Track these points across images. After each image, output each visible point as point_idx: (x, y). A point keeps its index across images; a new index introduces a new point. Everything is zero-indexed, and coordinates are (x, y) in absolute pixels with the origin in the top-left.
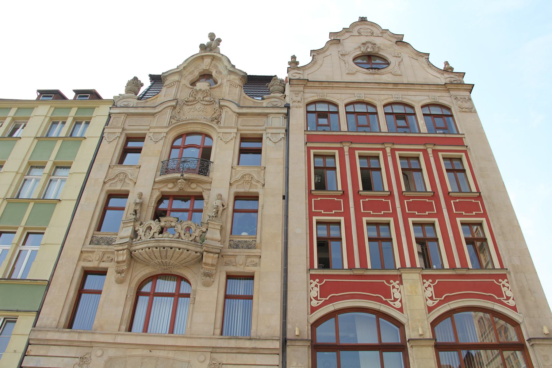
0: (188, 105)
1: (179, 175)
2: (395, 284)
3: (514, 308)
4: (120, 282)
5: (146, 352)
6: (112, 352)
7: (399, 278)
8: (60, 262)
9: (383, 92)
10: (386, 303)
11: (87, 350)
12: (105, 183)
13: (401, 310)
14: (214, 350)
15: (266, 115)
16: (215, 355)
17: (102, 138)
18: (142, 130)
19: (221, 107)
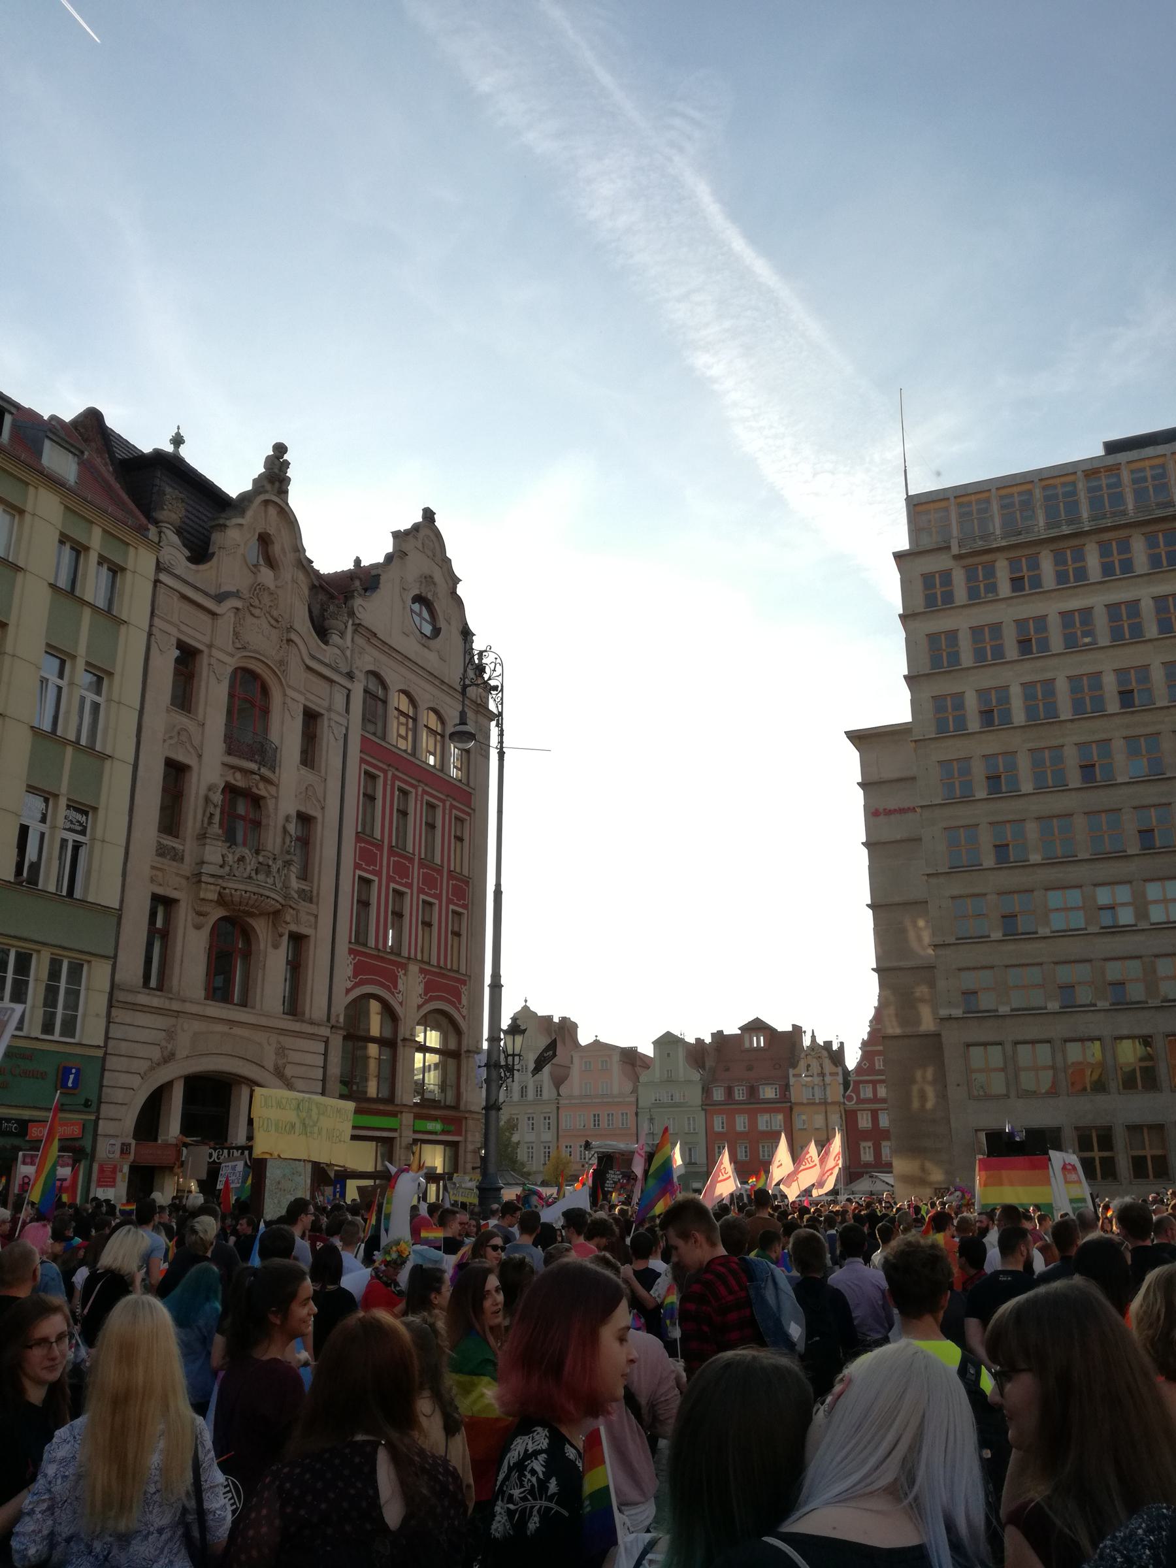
0: (252, 615)
1: (253, 766)
2: (402, 973)
3: (464, 1017)
4: (198, 927)
5: (224, 1028)
6: (197, 1026)
7: (404, 967)
8: (128, 880)
9: (428, 687)
10: (393, 994)
11: (172, 1021)
12: (164, 741)
13: (401, 1003)
14: (283, 1032)
15: (331, 681)
16: (281, 1038)
17: (150, 634)
18: (199, 641)
19: (289, 641)
